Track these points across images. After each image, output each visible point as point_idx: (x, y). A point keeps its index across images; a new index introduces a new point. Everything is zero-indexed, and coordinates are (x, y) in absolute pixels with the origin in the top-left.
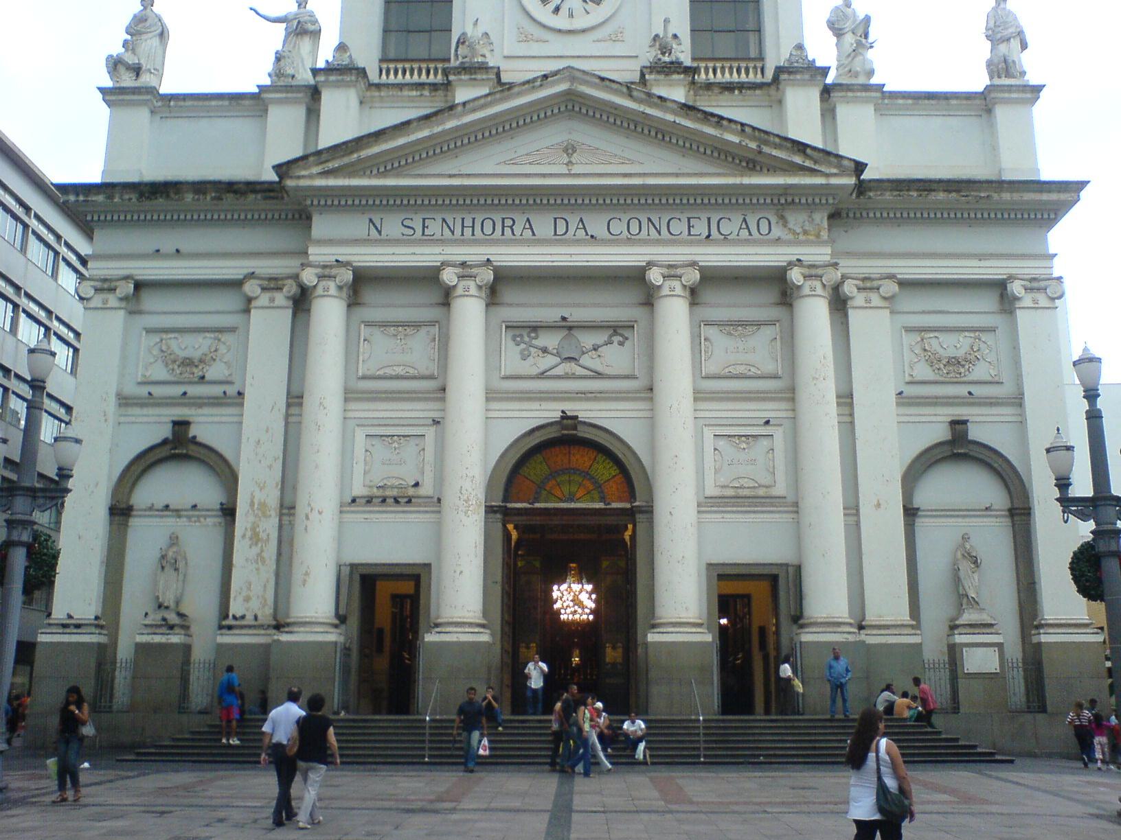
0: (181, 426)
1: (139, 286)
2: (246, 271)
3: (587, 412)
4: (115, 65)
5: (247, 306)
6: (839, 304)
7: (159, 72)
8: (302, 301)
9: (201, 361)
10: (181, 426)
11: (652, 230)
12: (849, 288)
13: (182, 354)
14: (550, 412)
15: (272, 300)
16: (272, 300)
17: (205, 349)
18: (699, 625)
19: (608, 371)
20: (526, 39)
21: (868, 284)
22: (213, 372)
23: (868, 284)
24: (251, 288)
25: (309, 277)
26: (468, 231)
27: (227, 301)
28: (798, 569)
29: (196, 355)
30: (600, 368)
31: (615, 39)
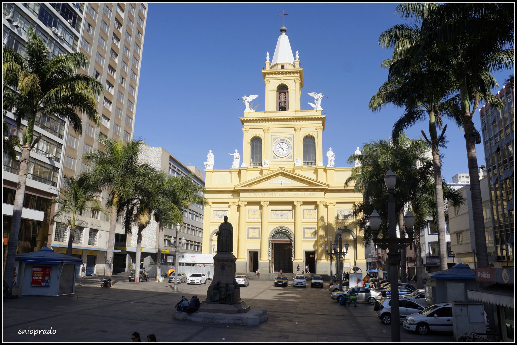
3: (285, 225)
5: (229, 207)
6: (326, 206)
8: (239, 207)
11: (295, 195)
12: (328, 204)
14: (279, 225)
16: (234, 206)
19: (288, 218)
20: (274, 158)
21: (331, 203)
23: (331, 203)
24: (230, 204)
25: (240, 203)
26: (265, 195)
30: (287, 217)
31: (289, 158)
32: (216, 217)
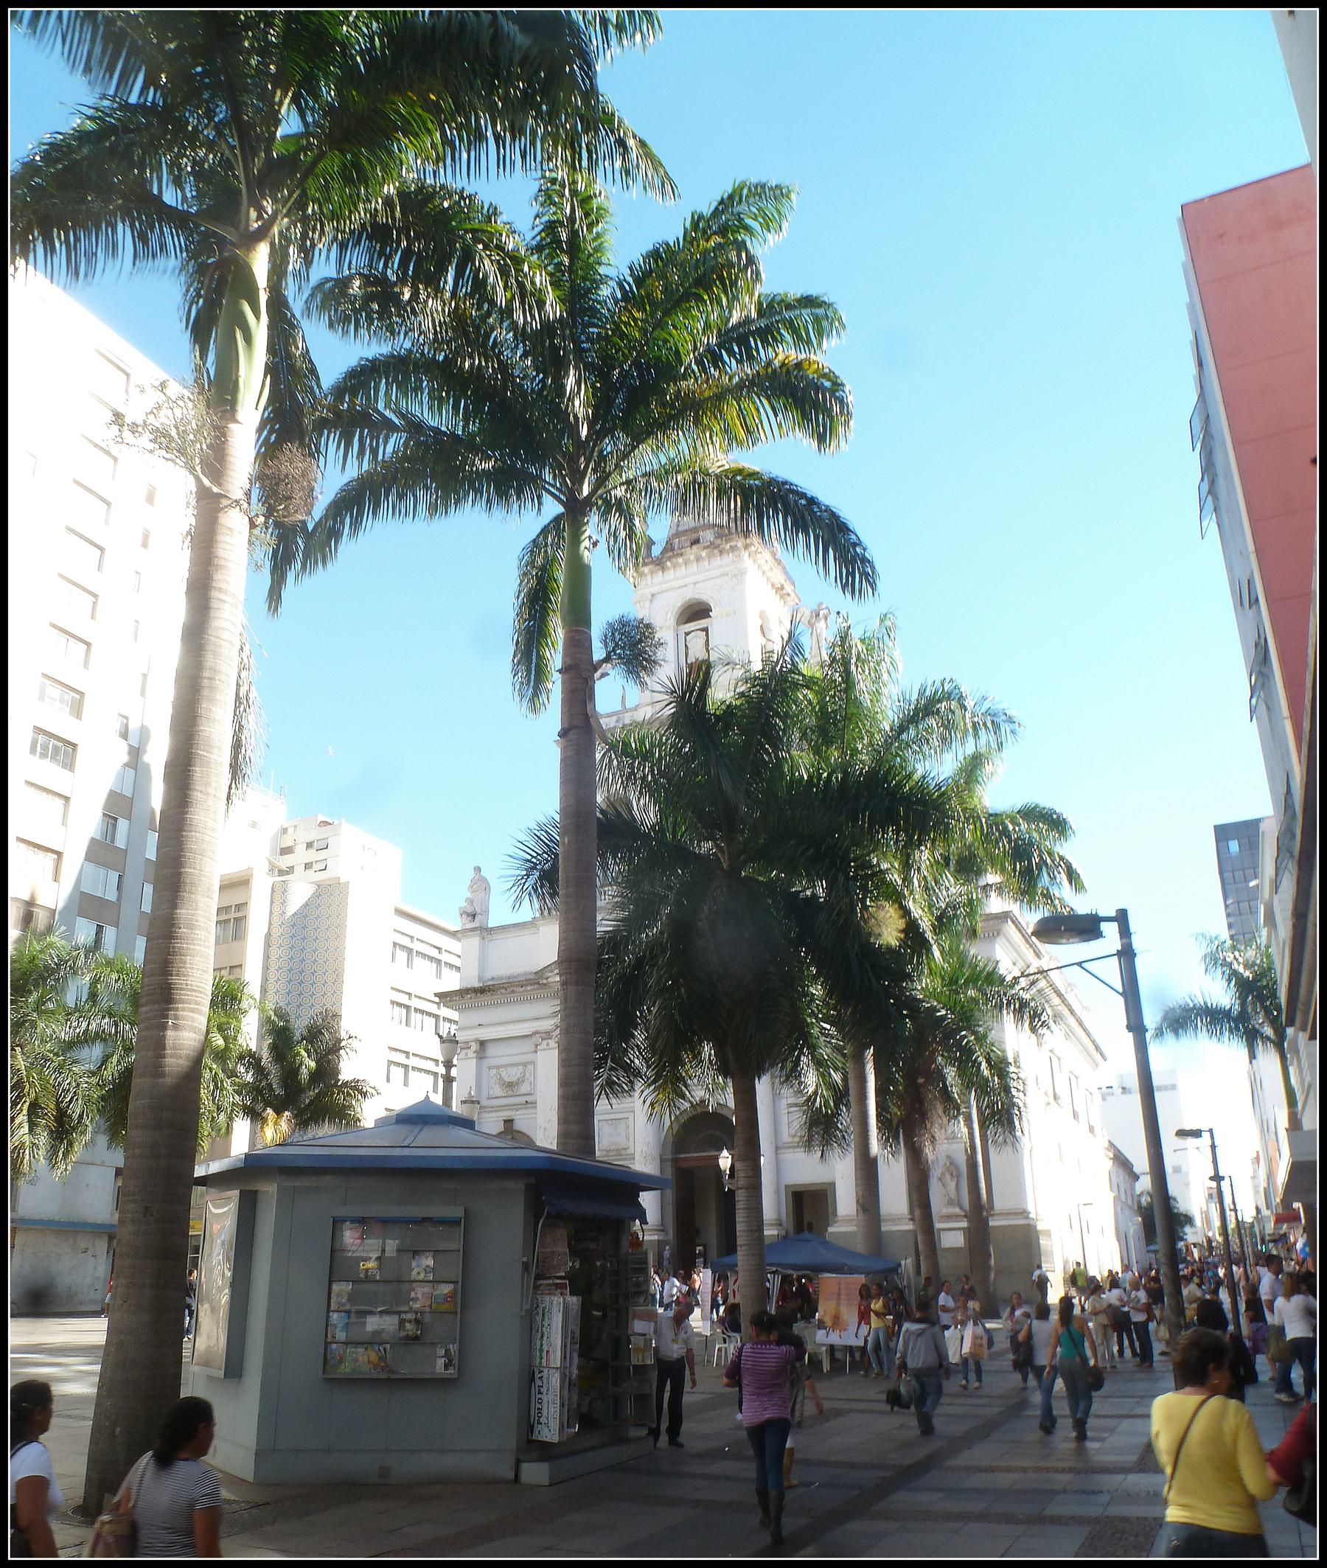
0: (508, 1122)
1: (482, 1043)
2: (535, 1029)
4: (464, 913)
7: (487, 912)
9: (517, 1083)
10: (508, 1122)
13: (508, 1080)
15: (548, 1045)
16: (548, 1045)
17: (518, 1075)
18: (781, 1225)
22: (525, 1088)
27: (528, 1046)
28: (835, 1184)
29: (514, 1079)
32: (498, 1091)
